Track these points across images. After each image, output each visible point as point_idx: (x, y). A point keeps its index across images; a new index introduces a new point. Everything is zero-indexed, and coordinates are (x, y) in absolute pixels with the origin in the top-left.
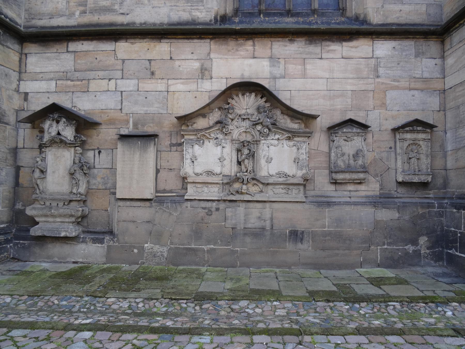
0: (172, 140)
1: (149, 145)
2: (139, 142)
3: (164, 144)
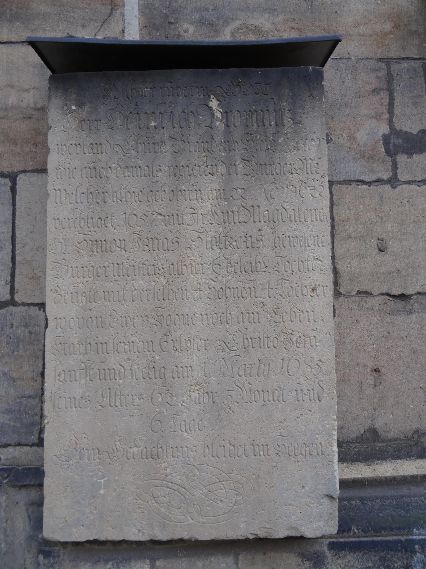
0: (397, 110)
1: (287, 120)
2: (214, 103)
3: (351, 138)
